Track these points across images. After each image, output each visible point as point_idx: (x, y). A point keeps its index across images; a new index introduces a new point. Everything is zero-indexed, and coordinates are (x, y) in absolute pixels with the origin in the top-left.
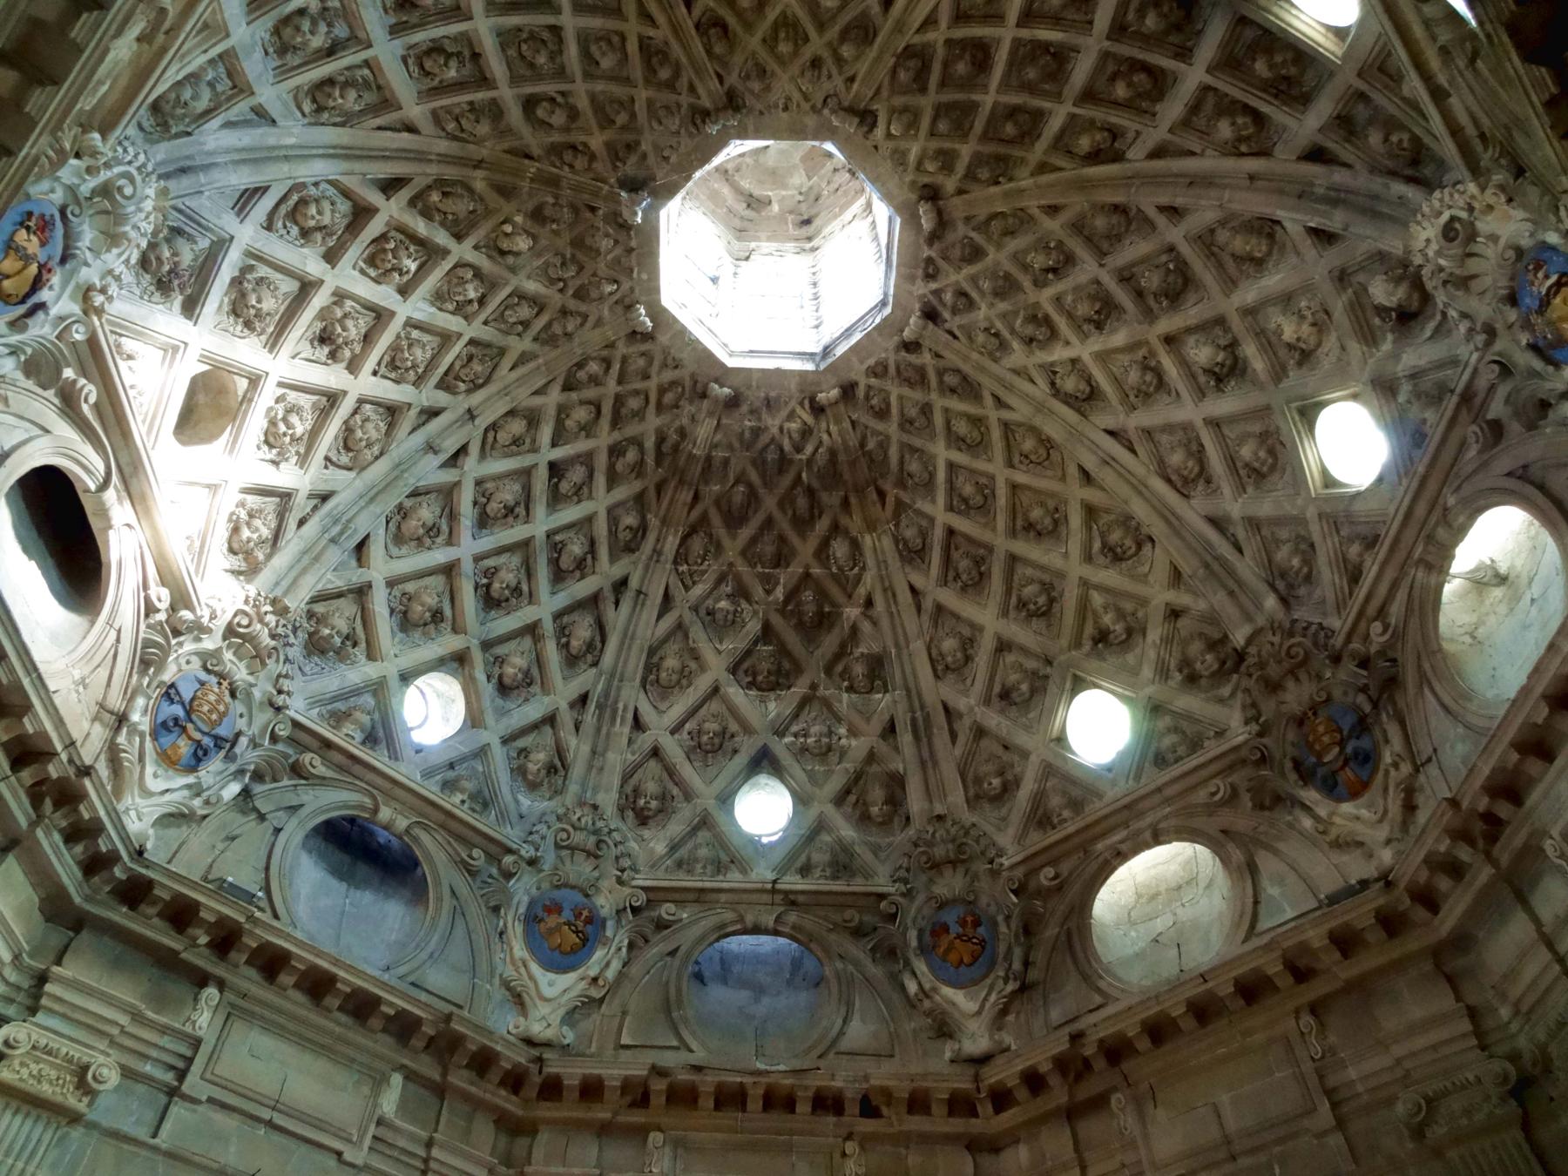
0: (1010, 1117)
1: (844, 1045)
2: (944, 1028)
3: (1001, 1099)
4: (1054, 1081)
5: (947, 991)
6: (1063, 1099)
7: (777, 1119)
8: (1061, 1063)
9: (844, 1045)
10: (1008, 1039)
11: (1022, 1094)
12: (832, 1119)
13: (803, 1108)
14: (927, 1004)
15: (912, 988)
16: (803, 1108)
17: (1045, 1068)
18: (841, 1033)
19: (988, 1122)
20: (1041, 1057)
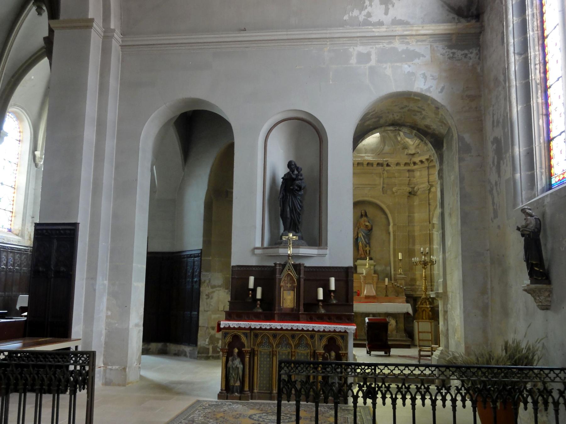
0: (416, 167)
1: (384, 151)
2: (405, 147)
3: (415, 163)
4: (426, 162)
5: (407, 139)
6: (427, 165)
7: (371, 168)
8: (427, 160)
9: (384, 151)
10: (418, 151)
11: (420, 163)
12: (380, 167)
13: (375, 166)
14: (402, 142)
15: (399, 139)
16: (375, 166)
17: (424, 160)
18: (383, 149)
19: (412, 167)
20: (423, 158)
